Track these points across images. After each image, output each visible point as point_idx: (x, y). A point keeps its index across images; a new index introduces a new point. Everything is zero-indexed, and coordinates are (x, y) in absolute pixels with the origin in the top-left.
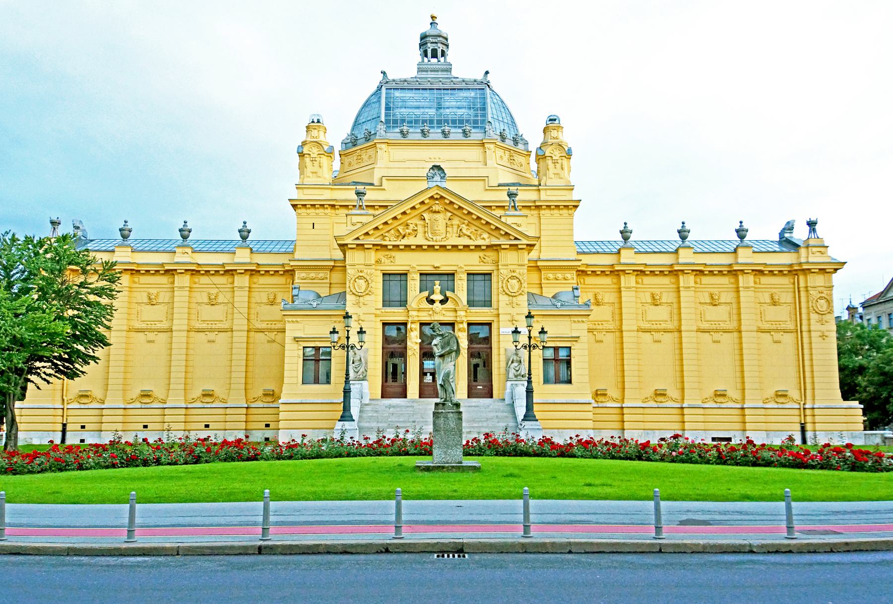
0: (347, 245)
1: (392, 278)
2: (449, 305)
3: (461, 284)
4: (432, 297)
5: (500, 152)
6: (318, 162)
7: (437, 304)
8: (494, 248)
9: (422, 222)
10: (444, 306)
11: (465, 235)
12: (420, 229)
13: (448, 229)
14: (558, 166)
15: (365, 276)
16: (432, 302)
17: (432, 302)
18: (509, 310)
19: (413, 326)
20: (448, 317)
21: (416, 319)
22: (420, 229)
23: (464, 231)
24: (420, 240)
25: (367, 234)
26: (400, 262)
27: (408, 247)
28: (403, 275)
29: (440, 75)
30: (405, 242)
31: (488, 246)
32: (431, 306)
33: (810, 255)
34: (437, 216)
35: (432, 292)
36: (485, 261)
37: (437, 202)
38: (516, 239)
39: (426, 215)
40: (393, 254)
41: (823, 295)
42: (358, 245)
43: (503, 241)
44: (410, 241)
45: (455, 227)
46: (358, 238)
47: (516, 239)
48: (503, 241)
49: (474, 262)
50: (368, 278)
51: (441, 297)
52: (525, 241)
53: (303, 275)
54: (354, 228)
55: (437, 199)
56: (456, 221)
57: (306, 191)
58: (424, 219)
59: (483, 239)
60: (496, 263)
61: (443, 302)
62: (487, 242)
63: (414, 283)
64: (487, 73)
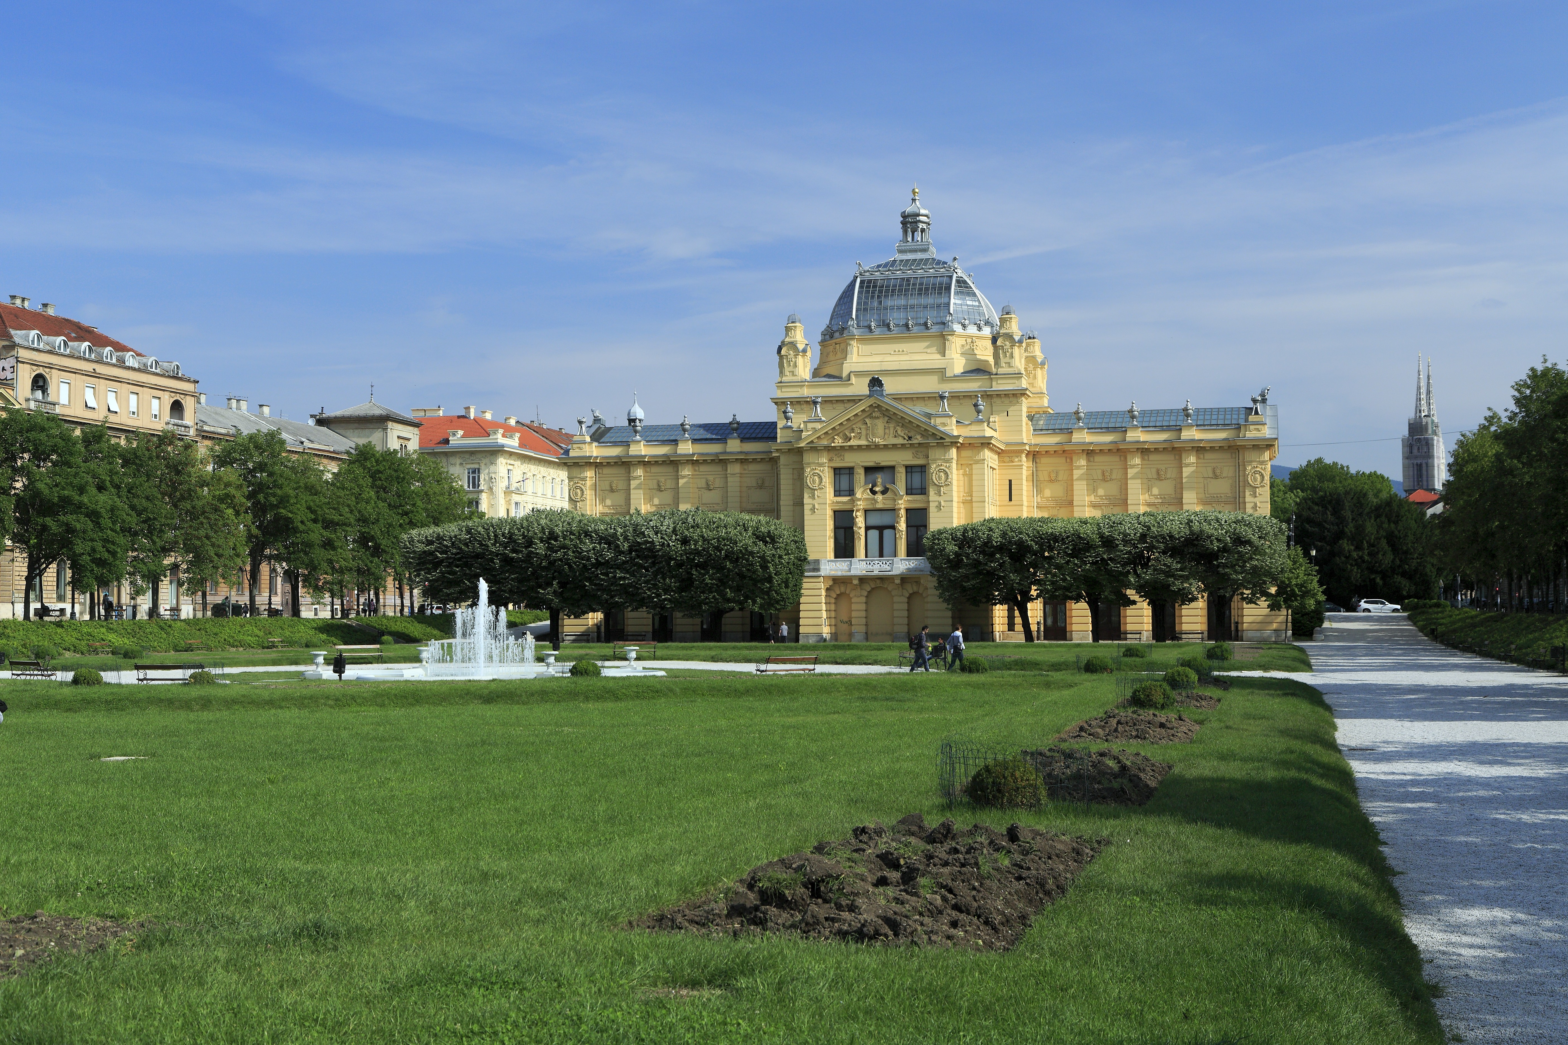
1: (842, 471)
2: (889, 494)
3: (901, 477)
9: (863, 427)
12: (864, 432)
13: (887, 431)
18: (937, 498)
23: (899, 432)
24: (863, 442)
26: (850, 459)
34: (877, 421)
35: (874, 485)
38: (942, 438)
39: (867, 421)
45: (892, 429)
46: (812, 442)
52: (948, 440)
56: (892, 425)
57: (783, 390)
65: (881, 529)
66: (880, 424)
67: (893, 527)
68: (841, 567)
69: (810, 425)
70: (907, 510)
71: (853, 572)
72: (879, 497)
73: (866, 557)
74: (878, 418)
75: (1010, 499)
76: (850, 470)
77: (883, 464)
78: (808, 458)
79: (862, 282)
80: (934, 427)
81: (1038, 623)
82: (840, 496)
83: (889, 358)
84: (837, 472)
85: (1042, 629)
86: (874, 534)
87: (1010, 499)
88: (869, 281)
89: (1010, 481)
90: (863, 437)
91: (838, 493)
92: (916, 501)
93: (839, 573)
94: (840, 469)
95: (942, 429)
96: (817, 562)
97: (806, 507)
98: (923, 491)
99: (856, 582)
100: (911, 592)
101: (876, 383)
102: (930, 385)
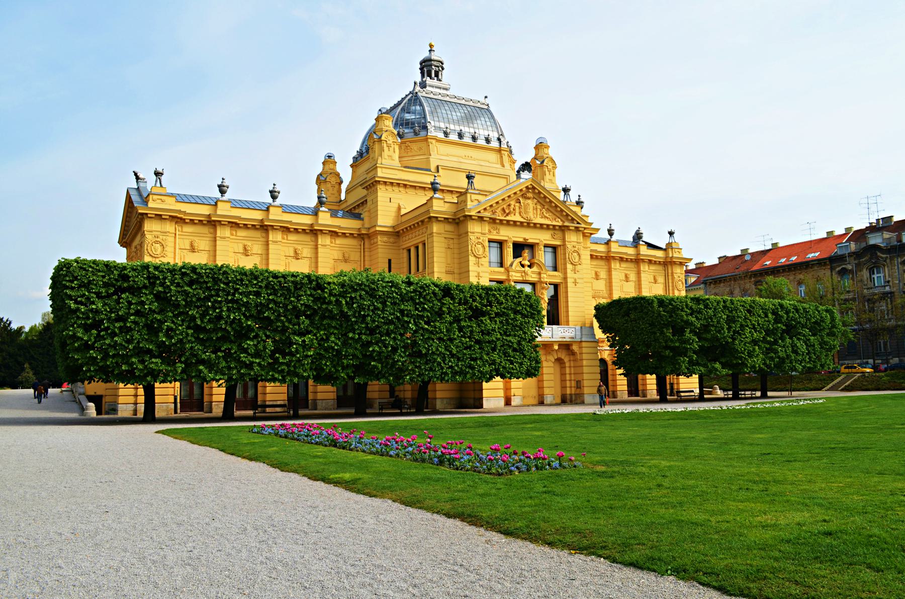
0: (470, 216)
7: (527, 269)
8: (563, 229)
10: (532, 270)
16: (523, 266)
17: (523, 266)
23: (545, 214)
24: (517, 218)
25: (485, 209)
27: (508, 221)
28: (501, 244)
29: (442, 91)
30: (508, 218)
31: (560, 226)
32: (523, 269)
36: (555, 237)
37: (530, 191)
40: (498, 227)
42: (479, 217)
44: (511, 218)
45: (539, 210)
47: (578, 223)
51: (529, 264)
53: (385, 239)
58: (520, 203)
59: (558, 221)
60: (564, 240)
61: (530, 266)
62: (560, 223)
63: (509, 251)
64: (486, 97)
74: (529, 198)
90: (517, 214)
92: (556, 277)
97: (471, 273)
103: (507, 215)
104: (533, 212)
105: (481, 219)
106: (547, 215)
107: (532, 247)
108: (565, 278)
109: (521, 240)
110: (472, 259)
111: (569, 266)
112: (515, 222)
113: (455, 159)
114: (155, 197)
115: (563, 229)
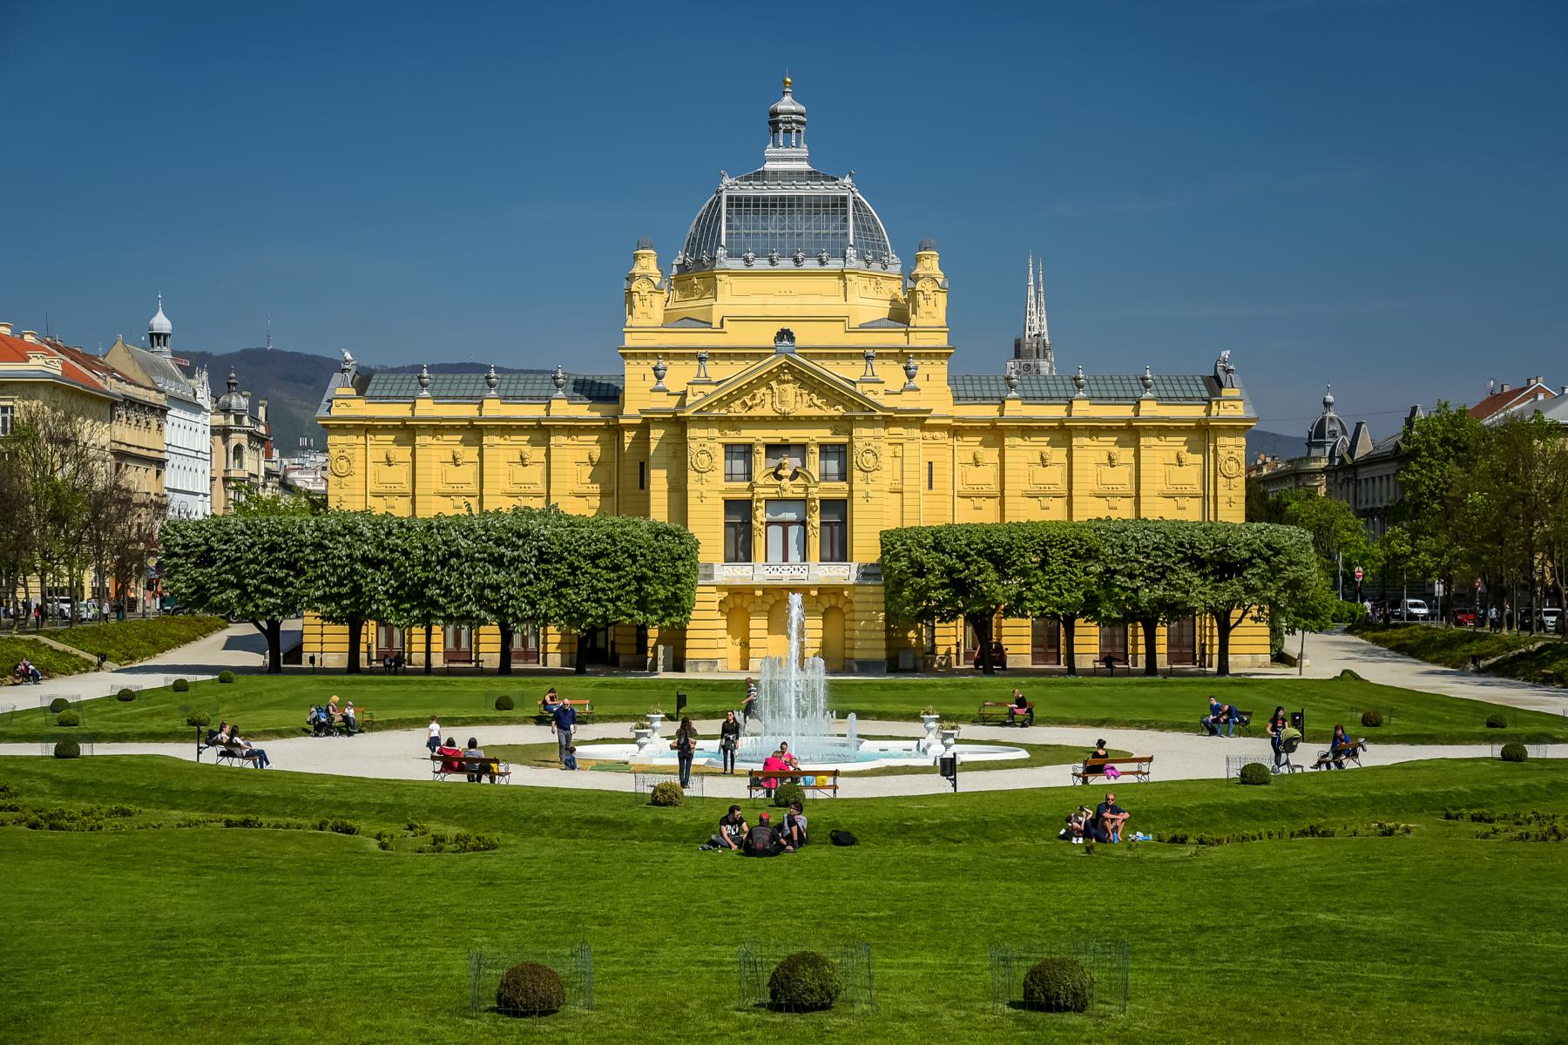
4: (779, 473)
5: (863, 282)
6: (648, 301)
11: (815, 405)
12: (768, 399)
14: (931, 302)
15: (708, 450)
16: (779, 478)
19: (758, 504)
20: (799, 493)
21: (762, 496)
22: (768, 399)
24: (767, 411)
27: (751, 419)
32: (778, 482)
33: (1221, 408)
38: (871, 410)
41: (1232, 455)
43: (857, 413)
46: (700, 410)
47: (871, 410)
48: (857, 413)
49: (824, 435)
50: (711, 452)
54: (697, 398)
55: (785, 368)
65: (785, 525)
66: (791, 389)
67: (803, 523)
68: (738, 574)
69: (697, 388)
70: (822, 501)
71: (757, 581)
72: (785, 482)
73: (766, 561)
74: (788, 382)
75: (931, 487)
76: (747, 451)
77: (792, 441)
78: (692, 432)
79: (729, 198)
80: (862, 397)
81: (958, 644)
82: (732, 480)
83: (771, 300)
84: (729, 449)
85: (962, 651)
86: (776, 532)
87: (931, 487)
88: (738, 198)
89: (930, 463)
91: (730, 476)
92: (837, 489)
93: (738, 582)
94: (732, 445)
95: (870, 396)
96: (710, 566)
98: (844, 475)
99: (759, 593)
100: (827, 606)
101: (785, 335)
102: (832, 336)
103: (750, 408)
104: (794, 400)
105: (704, 421)
106: (818, 402)
107: (801, 449)
108: (851, 491)
109: (778, 441)
110: (691, 474)
111: (857, 474)
112: (763, 422)
113: (759, 300)
114: (339, 402)
115: (844, 424)
